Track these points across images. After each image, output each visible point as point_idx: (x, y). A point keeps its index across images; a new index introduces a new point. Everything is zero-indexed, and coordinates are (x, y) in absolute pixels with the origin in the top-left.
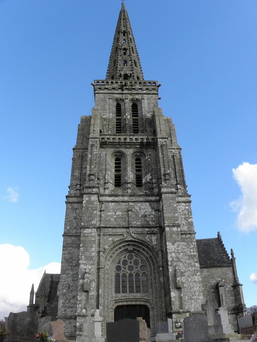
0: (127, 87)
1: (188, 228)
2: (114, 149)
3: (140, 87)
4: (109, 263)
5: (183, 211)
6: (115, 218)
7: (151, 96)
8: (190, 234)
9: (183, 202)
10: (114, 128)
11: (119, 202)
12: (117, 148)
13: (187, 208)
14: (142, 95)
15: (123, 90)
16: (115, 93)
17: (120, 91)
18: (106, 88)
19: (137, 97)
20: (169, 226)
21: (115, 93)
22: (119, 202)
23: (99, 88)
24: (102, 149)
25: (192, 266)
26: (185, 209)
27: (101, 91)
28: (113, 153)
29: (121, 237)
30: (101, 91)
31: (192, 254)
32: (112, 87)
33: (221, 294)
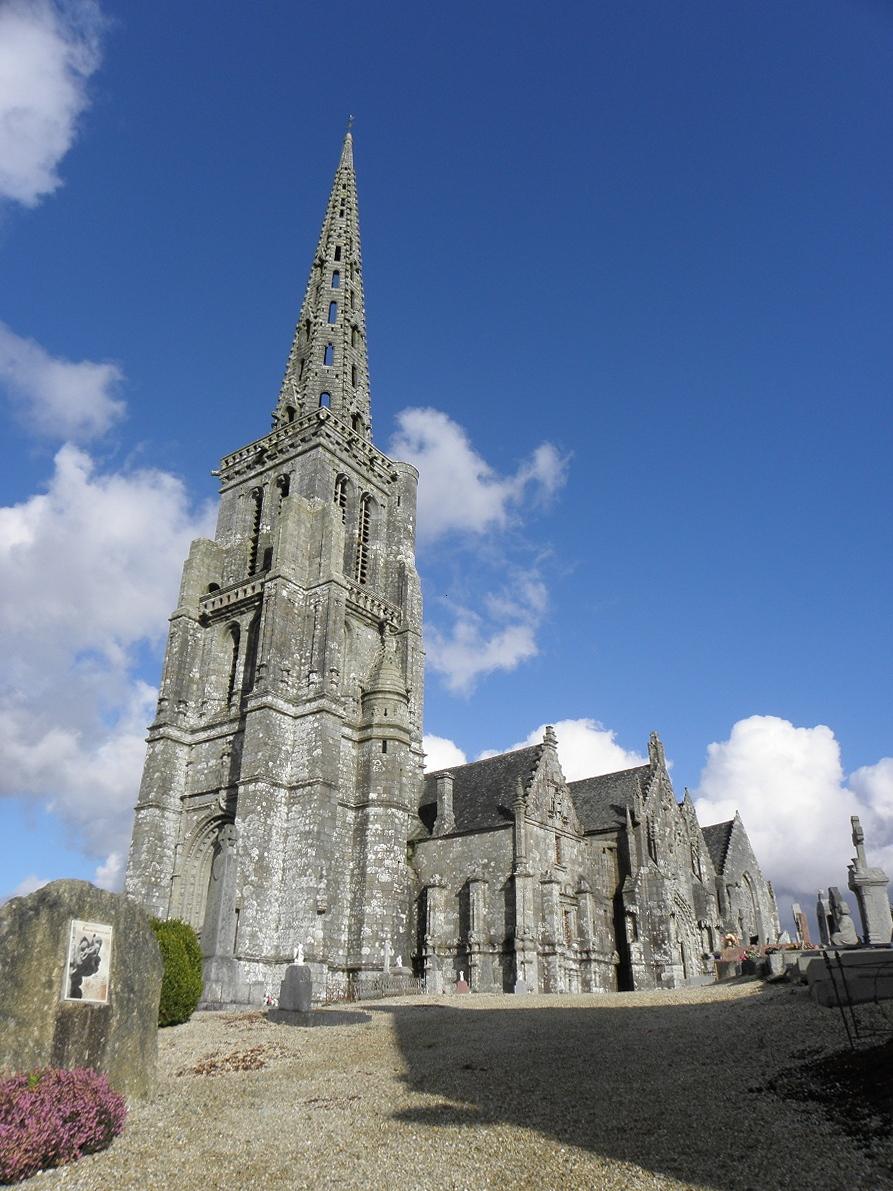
0: (269, 453)
1: (310, 771)
2: (225, 623)
3: (290, 443)
4: (197, 864)
5: (308, 735)
6: (206, 775)
7: (308, 454)
8: (310, 784)
9: (311, 714)
10: (245, 564)
11: (214, 739)
12: (227, 618)
13: (316, 725)
14: (292, 461)
15: (264, 463)
16: (250, 479)
17: (259, 468)
18: (237, 473)
19: (285, 469)
20: (243, 783)
21: (250, 479)
22: (214, 739)
23: (227, 478)
24: (208, 629)
25: (302, 856)
26: (312, 729)
27: (232, 483)
28: (226, 631)
29: (208, 812)
30: (232, 483)
31: (307, 828)
32: (245, 464)
33: (471, 901)
